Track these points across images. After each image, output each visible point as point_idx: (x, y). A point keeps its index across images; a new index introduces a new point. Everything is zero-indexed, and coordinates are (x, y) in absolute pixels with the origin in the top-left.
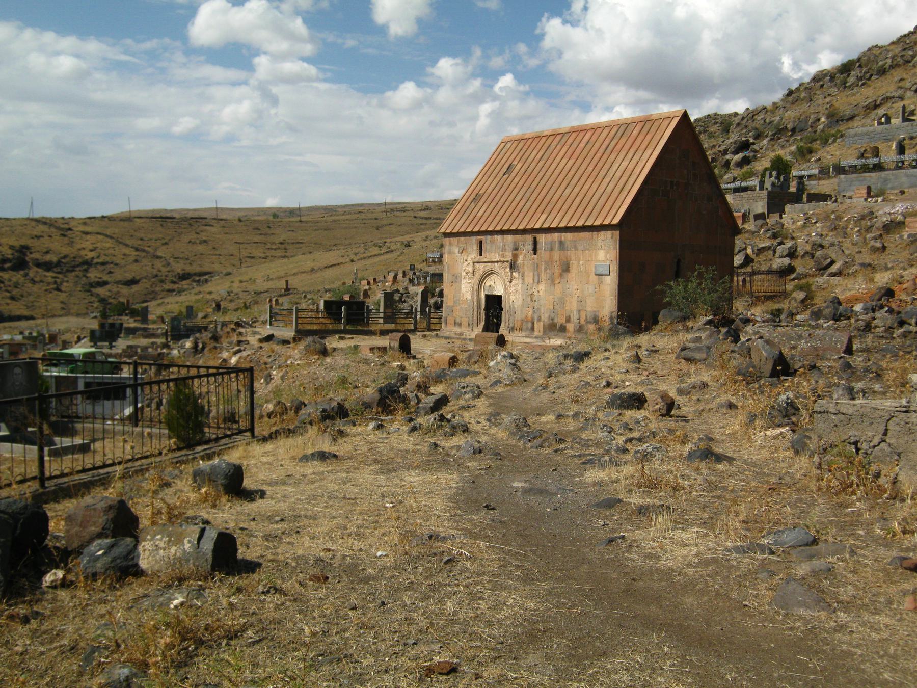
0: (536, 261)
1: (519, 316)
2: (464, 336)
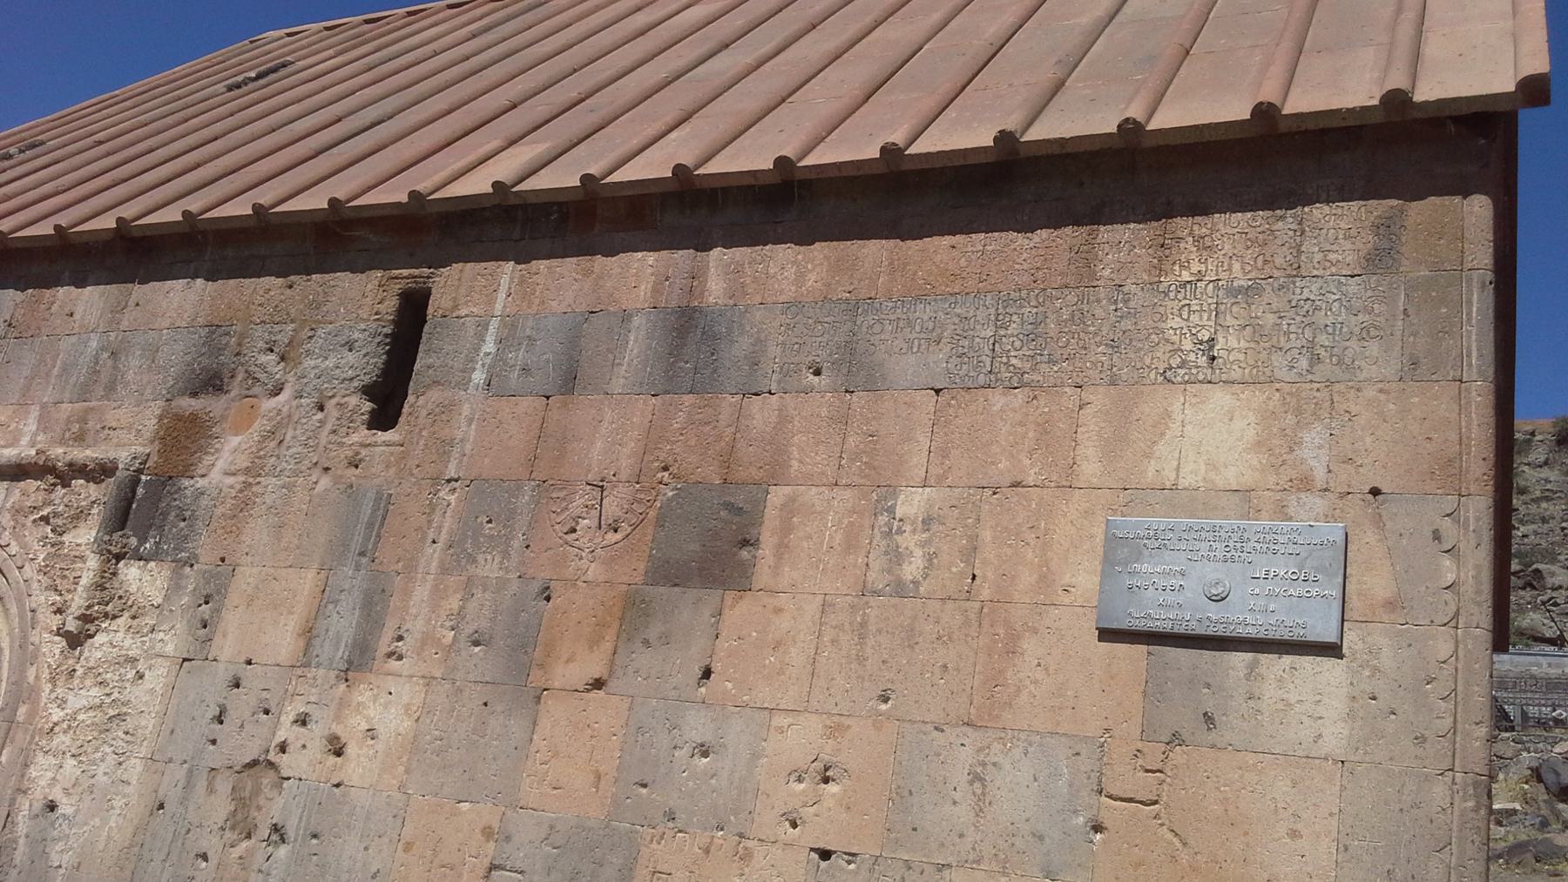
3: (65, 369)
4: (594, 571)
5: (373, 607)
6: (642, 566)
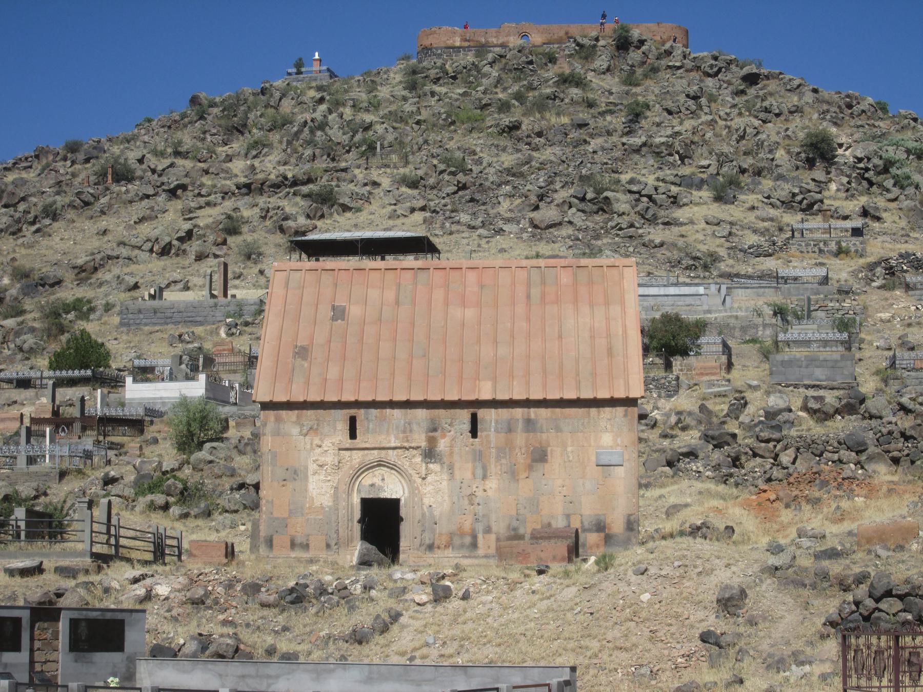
0: (478, 448)
1: (444, 527)
3: (397, 427)
4: (522, 461)
5: (485, 469)
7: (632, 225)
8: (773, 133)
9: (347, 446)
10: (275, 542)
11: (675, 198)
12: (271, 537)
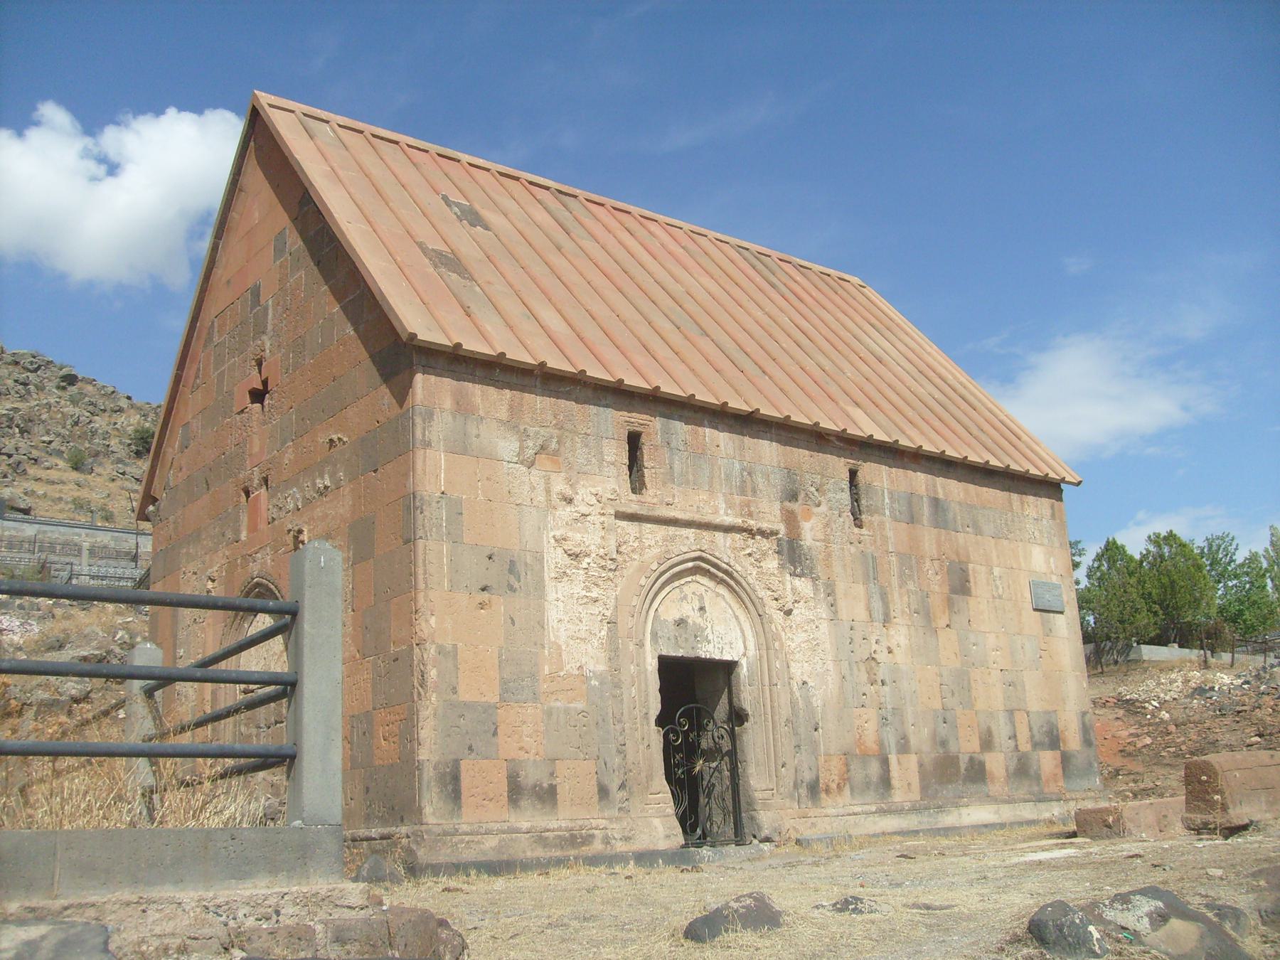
1: (832, 739)
2: (597, 846)
3: (728, 477)
4: (937, 588)
5: (884, 597)
6: (948, 587)
7: (5, 476)
8: (104, 424)
9: (633, 508)
10: (465, 782)
11: (36, 460)
12: (456, 763)
